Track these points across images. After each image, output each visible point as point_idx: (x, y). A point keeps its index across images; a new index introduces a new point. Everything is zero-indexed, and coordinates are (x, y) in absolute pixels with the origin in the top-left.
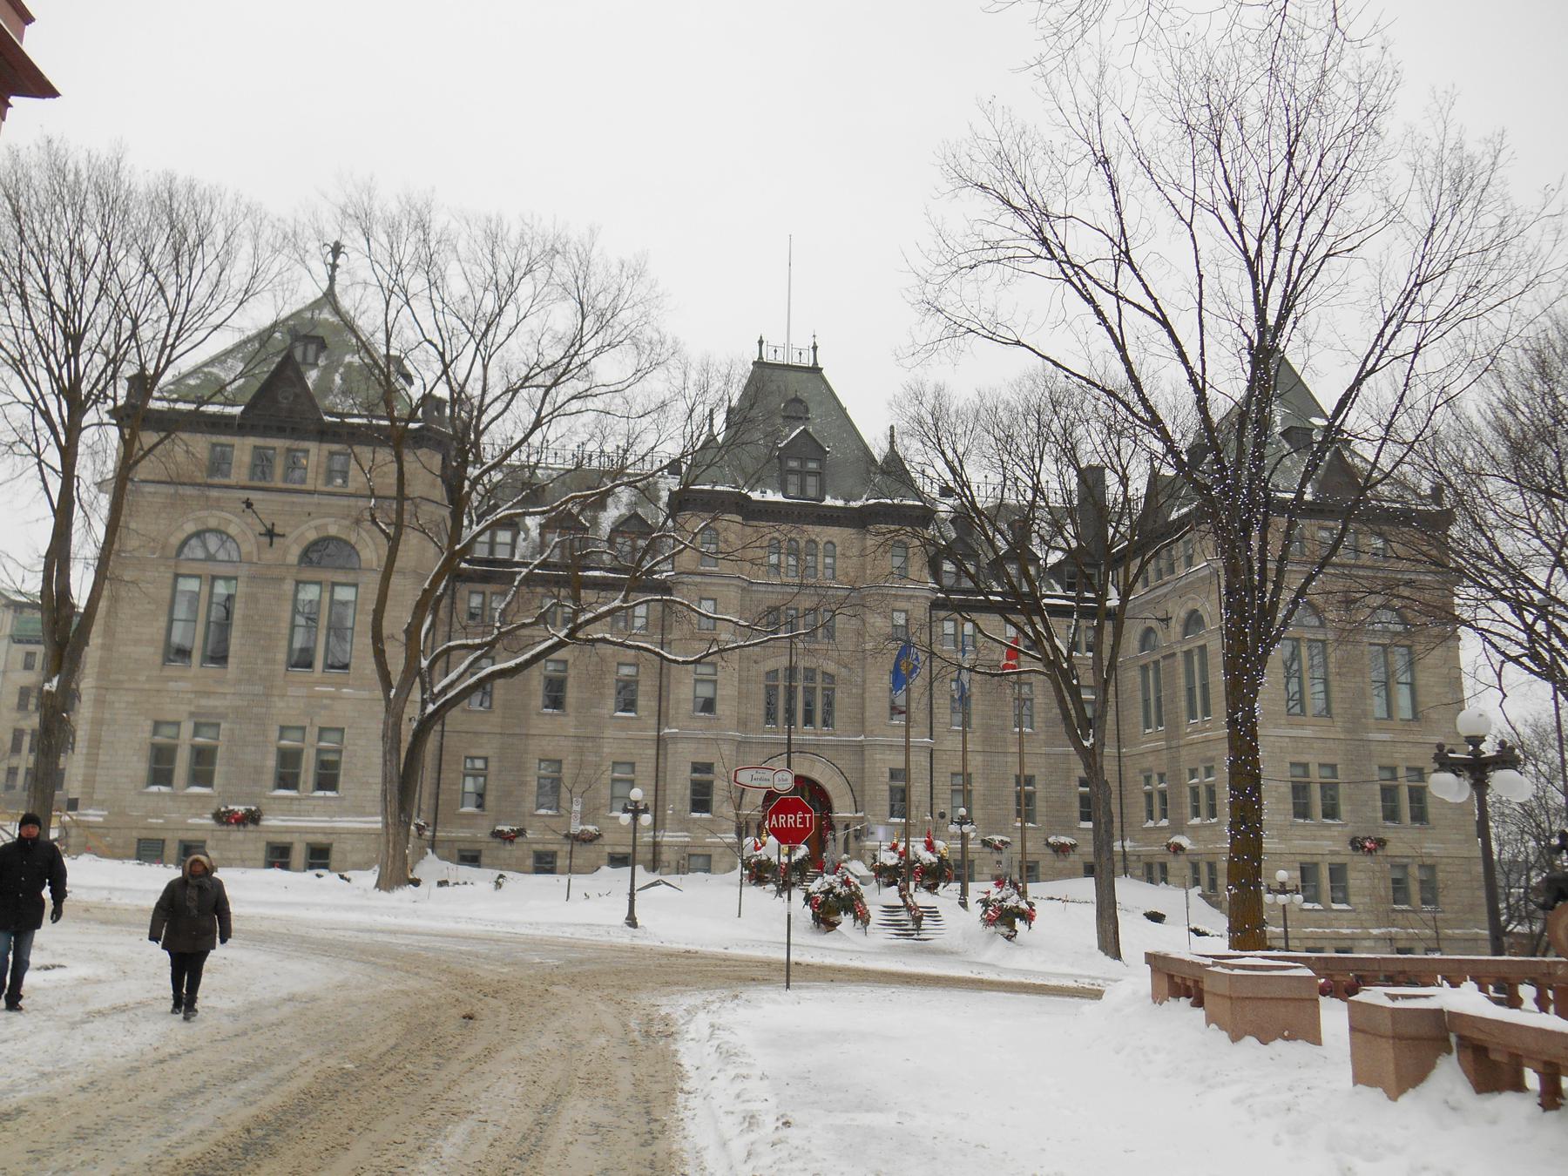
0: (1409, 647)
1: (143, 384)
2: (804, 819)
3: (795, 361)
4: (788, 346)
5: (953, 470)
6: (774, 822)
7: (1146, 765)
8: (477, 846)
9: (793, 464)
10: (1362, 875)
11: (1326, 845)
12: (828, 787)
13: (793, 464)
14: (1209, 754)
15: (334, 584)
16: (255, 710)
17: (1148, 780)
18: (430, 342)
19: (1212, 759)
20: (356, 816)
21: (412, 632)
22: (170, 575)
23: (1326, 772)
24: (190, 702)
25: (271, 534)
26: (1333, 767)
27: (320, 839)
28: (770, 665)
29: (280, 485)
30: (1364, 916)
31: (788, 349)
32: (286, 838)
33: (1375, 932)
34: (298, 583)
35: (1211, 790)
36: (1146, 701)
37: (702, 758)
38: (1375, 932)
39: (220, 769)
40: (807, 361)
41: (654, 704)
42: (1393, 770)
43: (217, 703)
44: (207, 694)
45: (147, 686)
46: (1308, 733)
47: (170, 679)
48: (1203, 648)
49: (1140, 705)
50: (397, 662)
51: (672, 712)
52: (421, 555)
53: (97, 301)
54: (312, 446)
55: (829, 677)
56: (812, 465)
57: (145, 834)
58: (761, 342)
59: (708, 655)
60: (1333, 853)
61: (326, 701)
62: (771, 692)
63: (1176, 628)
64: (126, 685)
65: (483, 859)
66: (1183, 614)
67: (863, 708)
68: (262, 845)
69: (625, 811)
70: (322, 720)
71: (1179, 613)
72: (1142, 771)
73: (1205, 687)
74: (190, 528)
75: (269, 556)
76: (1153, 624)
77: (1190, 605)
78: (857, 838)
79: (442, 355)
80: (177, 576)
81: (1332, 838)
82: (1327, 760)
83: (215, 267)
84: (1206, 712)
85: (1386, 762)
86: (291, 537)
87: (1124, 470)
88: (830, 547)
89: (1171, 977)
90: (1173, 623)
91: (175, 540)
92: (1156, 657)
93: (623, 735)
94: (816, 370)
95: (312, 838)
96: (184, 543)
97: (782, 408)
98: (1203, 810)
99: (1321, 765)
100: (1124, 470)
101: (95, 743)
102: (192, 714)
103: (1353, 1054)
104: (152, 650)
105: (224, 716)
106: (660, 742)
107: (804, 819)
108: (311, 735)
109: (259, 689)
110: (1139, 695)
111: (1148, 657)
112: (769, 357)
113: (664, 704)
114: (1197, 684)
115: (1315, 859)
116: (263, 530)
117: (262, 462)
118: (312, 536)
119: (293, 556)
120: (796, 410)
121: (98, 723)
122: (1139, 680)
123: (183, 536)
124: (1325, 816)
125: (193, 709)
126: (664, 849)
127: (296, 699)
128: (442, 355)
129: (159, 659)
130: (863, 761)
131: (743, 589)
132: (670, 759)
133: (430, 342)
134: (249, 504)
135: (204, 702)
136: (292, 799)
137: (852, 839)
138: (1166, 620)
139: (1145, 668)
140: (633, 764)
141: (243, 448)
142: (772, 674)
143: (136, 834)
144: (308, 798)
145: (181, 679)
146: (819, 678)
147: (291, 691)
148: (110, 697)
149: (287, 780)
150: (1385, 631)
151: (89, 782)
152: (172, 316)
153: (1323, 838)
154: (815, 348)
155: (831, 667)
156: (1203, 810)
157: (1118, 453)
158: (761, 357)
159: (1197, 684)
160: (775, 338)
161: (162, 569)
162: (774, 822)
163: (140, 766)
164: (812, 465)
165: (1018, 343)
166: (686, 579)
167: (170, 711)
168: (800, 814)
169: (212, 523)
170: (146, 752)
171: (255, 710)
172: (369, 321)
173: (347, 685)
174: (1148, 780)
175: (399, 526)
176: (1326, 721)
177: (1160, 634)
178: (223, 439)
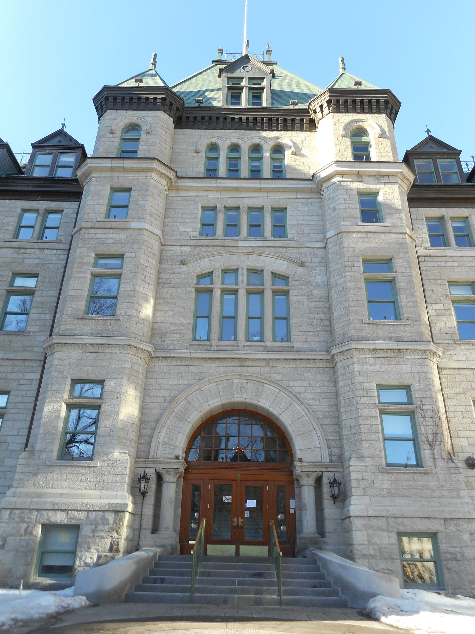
28: (205, 265)
78: (334, 498)
137: (327, 502)
146: (267, 278)
154: (269, 52)
155: (281, 266)
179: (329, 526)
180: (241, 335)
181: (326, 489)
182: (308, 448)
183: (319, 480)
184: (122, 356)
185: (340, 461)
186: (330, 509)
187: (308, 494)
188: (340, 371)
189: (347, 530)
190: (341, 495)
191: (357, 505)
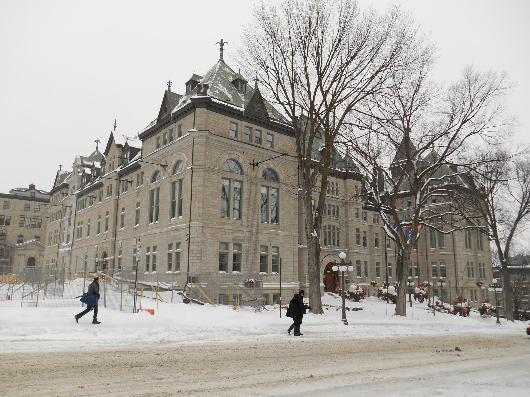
14: (443, 258)
16: (254, 238)
19: (445, 260)
37: (358, 259)
39: (243, 264)
43: (241, 235)
44: (237, 231)
45: (217, 227)
46: (469, 254)
55: (338, 229)
61: (274, 236)
64: (210, 226)
70: (273, 244)
102: (233, 240)
104: (217, 210)
105: (243, 241)
109: (254, 230)
127: (268, 234)
135: (237, 234)
136: (267, 276)
144: (272, 275)
149: (263, 268)
161: (219, 174)
167: (228, 238)
171: (254, 238)
173: (280, 230)
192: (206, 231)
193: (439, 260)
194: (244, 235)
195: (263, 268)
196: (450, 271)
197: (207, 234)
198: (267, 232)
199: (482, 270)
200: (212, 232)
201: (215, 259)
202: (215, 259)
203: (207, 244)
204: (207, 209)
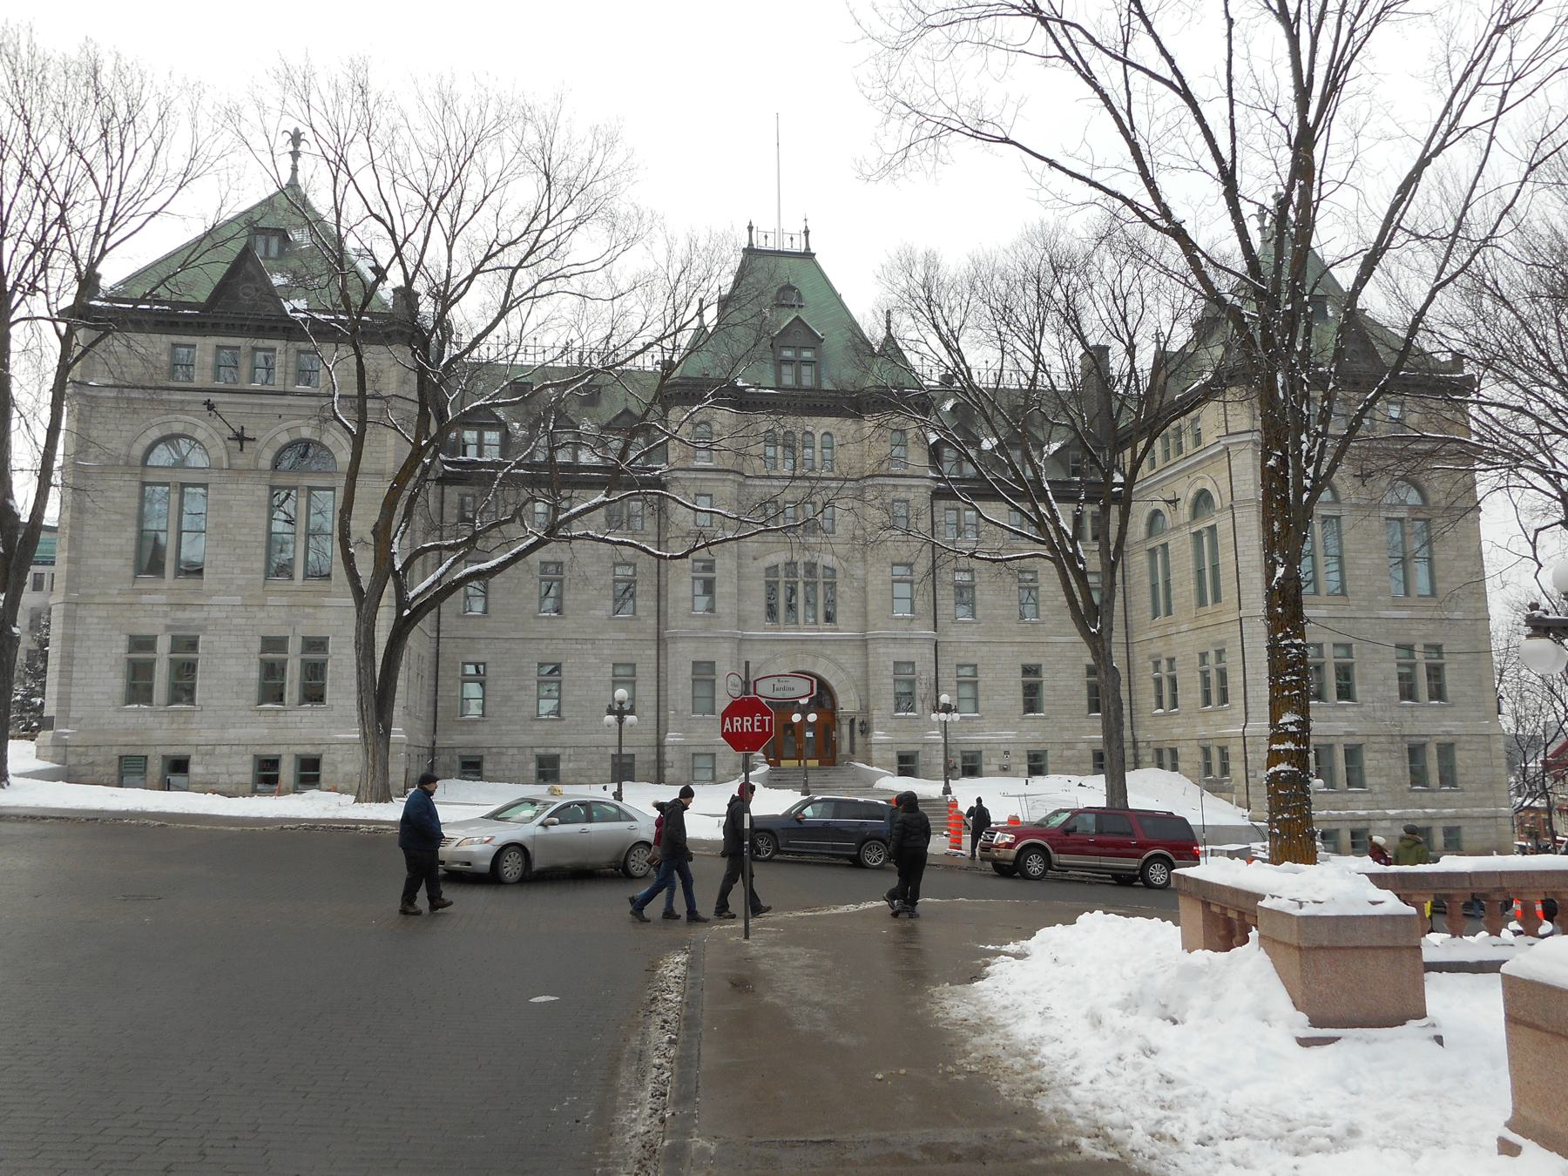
0: (1427, 521)
1: (88, 281)
2: (762, 722)
3: (787, 247)
4: (780, 232)
5: (947, 346)
6: (728, 725)
7: (1154, 651)
8: (478, 752)
9: (788, 354)
10: (1379, 756)
11: (1342, 727)
12: (833, 682)
13: (788, 354)
14: (1220, 637)
15: (311, 489)
17: (1157, 664)
18: (378, 218)
19: (1223, 642)
20: (335, 726)
21: (382, 534)
22: (137, 484)
23: (1341, 652)
24: (166, 615)
25: (240, 438)
26: (1348, 647)
27: (309, 750)
28: (772, 559)
29: (247, 387)
30: (1381, 797)
31: (779, 234)
32: (275, 751)
33: (1391, 812)
34: (272, 488)
35: (1223, 675)
36: (1154, 587)
38: (1391, 812)
40: (798, 246)
41: (653, 604)
42: (1410, 648)
43: (195, 615)
44: (182, 606)
45: (119, 600)
47: (141, 592)
48: (1213, 529)
49: (1148, 590)
50: (365, 569)
51: (670, 611)
52: (388, 450)
53: (20, 182)
54: (279, 344)
56: (807, 354)
57: (125, 751)
58: (750, 228)
59: (695, 549)
60: (1349, 734)
61: (311, 610)
62: (772, 588)
63: (1185, 509)
65: (487, 766)
66: (1191, 495)
67: (865, 603)
68: (249, 758)
69: (610, 711)
71: (1187, 494)
72: (1150, 657)
73: (1215, 568)
74: (155, 433)
75: (241, 461)
76: (1161, 506)
77: (1199, 485)
78: (862, 732)
79: (392, 233)
80: (144, 484)
81: (1348, 719)
82: (1344, 639)
83: (148, 150)
84: (1217, 598)
85: (1404, 640)
86: (263, 441)
87: (1131, 338)
88: (827, 438)
89: (1206, 905)
90: (1180, 504)
91: (138, 451)
92: (1163, 541)
93: (623, 636)
94: (808, 255)
95: (301, 750)
96: (150, 449)
97: (774, 291)
98: (1214, 697)
99: (1335, 645)
100: (1131, 338)
101: (68, 659)
102: (168, 628)
103: (1511, 1058)
104: (121, 562)
106: (660, 642)
107: (762, 722)
108: (294, 646)
110: (1147, 580)
111: (1155, 543)
112: (759, 243)
113: (663, 603)
114: (1207, 565)
115: (1330, 740)
116: (231, 434)
117: (225, 363)
118: (284, 439)
119: (266, 462)
120: (787, 295)
121: (68, 639)
122: (1146, 564)
123: (148, 442)
124: (1339, 698)
125: (168, 622)
126: (668, 749)
128: (392, 233)
129: (130, 572)
130: (866, 655)
131: (740, 484)
132: (671, 660)
133: (378, 218)
134: (210, 406)
135: (180, 615)
137: (857, 734)
138: (1174, 502)
139: (1152, 551)
140: (633, 665)
141: (205, 348)
142: (773, 569)
143: (115, 751)
145: (155, 591)
146: (819, 571)
147: (271, 600)
148: (81, 612)
150: (1403, 503)
151: (64, 700)
152: (104, 201)
153: (1340, 719)
154: (807, 232)
155: (828, 560)
156: (1214, 697)
157: (1124, 319)
158: (751, 244)
159: (1207, 565)
160: (765, 224)
162: (728, 725)
163: (116, 682)
164: (807, 354)
165: (1006, 140)
166: (678, 474)
168: (758, 717)
169: (178, 428)
170: (122, 668)
171: (235, 621)
172: (321, 202)
174: (1157, 664)
175: (362, 423)
176: (1341, 600)
177: (1168, 516)
178: (185, 339)
179: (858, 748)
180: (801, 620)
181: (857, 726)
182: (847, 703)
183: (852, 721)
184: (726, 645)
185: (866, 709)
186: (858, 739)
187: (845, 730)
188: (871, 651)
189: (869, 751)
190: (866, 730)
191: (878, 736)
192: (84, 613)
193: (1213, 644)
194: (204, 615)
195: (272, 692)
196: (1235, 680)
197: (89, 620)
198: (284, 601)
199: (1422, 672)
200: (104, 614)
201: (111, 674)
202: (111, 674)
203: (90, 643)
204: (90, 562)
